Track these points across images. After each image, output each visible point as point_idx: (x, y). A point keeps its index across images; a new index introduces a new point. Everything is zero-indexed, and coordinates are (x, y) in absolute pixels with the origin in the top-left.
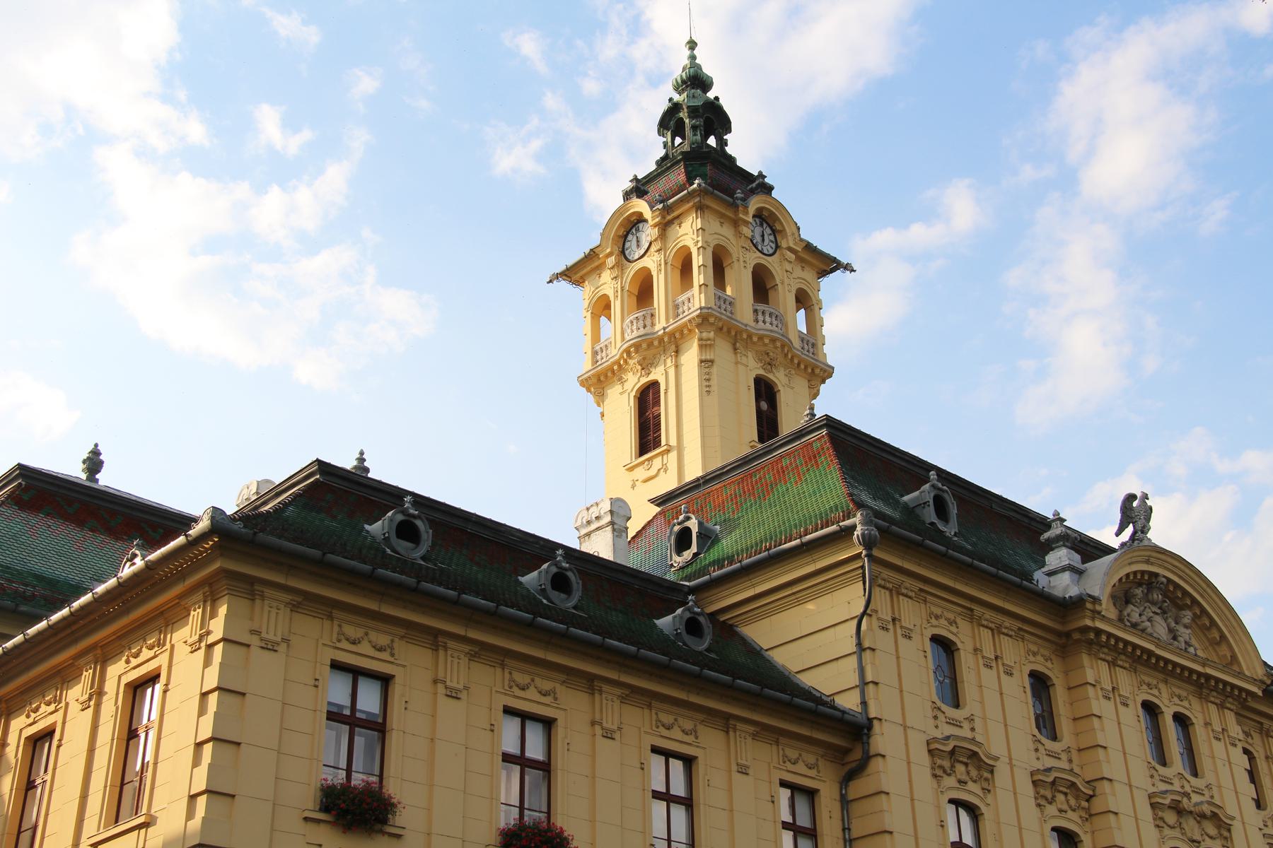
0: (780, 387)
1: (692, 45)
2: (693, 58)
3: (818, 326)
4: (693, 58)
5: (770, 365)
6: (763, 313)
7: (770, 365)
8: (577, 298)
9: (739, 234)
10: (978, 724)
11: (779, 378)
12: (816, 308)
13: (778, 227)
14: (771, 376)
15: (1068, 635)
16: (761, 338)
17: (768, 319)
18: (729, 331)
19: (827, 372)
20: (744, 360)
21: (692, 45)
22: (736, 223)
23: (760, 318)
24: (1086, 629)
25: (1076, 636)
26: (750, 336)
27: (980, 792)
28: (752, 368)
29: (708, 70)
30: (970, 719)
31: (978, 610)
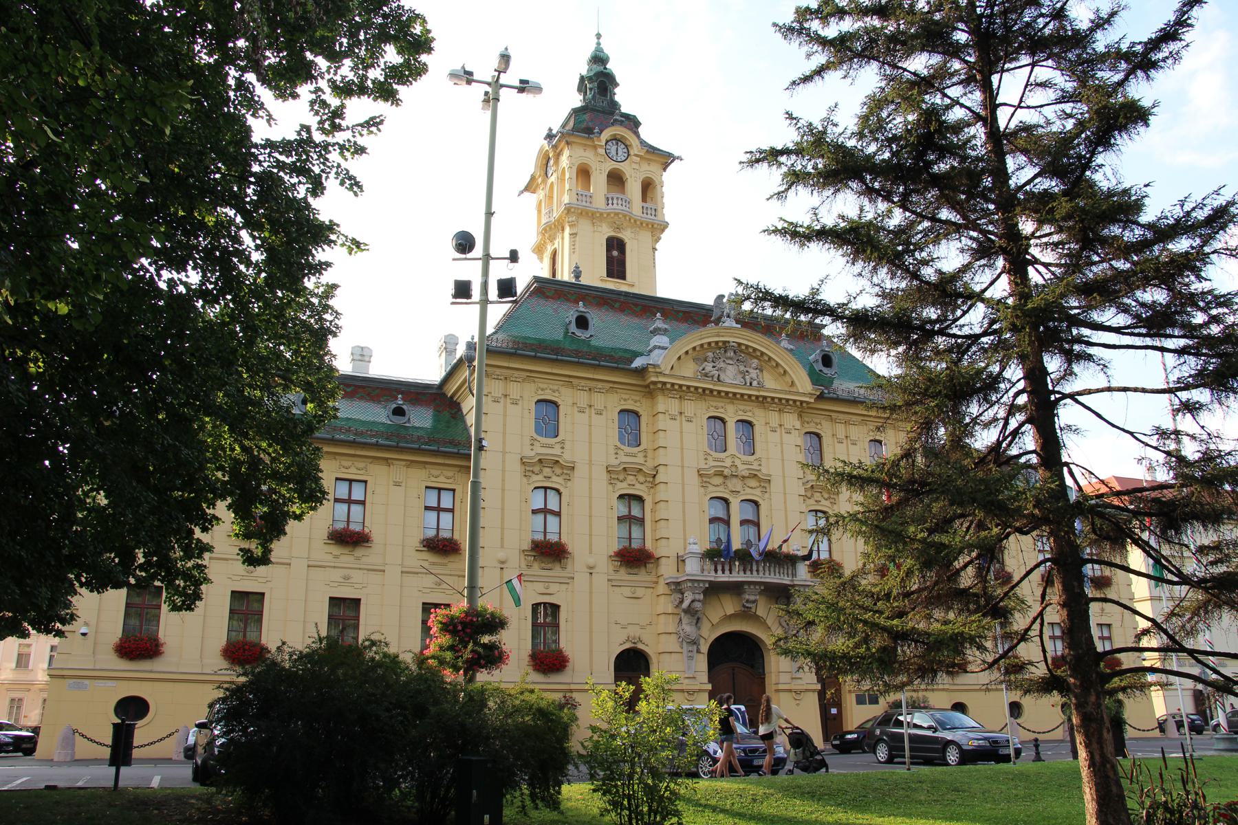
0: (626, 240)
1: (599, 36)
2: (599, 44)
3: (659, 198)
4: (599, 44)
5: (618, 228)
6: (612, 199)
7: (618, 228)
8: (531, 199)
9: (597, 154)
10: (567, 446)
11: (626, 236)
12: (658, 187)
13: (628, 143)
14: (620, 235)
15: (647, 386)
16: (608, 214)
17: (620, 202)
18: (587, 213)
19: (664, 226)
20: (600, 229)
21: (599, 36)
22: (595, 147)
23: (610, 202)
24: (655, 383)
25: (652, 387)
26: (601, 214)
27: (563, 482)
28: (607, 232)
29: (607, 49)
30: (562, 442)
31: (575, 381)
